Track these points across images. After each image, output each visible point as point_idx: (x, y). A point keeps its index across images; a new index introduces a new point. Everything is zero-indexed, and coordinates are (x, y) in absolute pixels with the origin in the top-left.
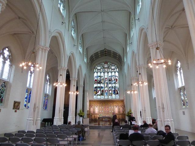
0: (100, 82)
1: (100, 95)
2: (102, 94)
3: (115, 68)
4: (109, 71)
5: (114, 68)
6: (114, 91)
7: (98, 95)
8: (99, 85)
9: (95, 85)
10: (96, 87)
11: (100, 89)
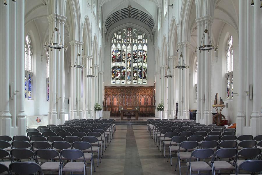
0: (119, 60)
1: (120, 80)
2: (123, 78)
3: (143, 38)
4: (133, 42)
5: (141, 38)
6: (141, 73)
7: (117, 79)
8: (118, 64)
9: (113, 65)
10: (114, 68)
11: (120, 71)
